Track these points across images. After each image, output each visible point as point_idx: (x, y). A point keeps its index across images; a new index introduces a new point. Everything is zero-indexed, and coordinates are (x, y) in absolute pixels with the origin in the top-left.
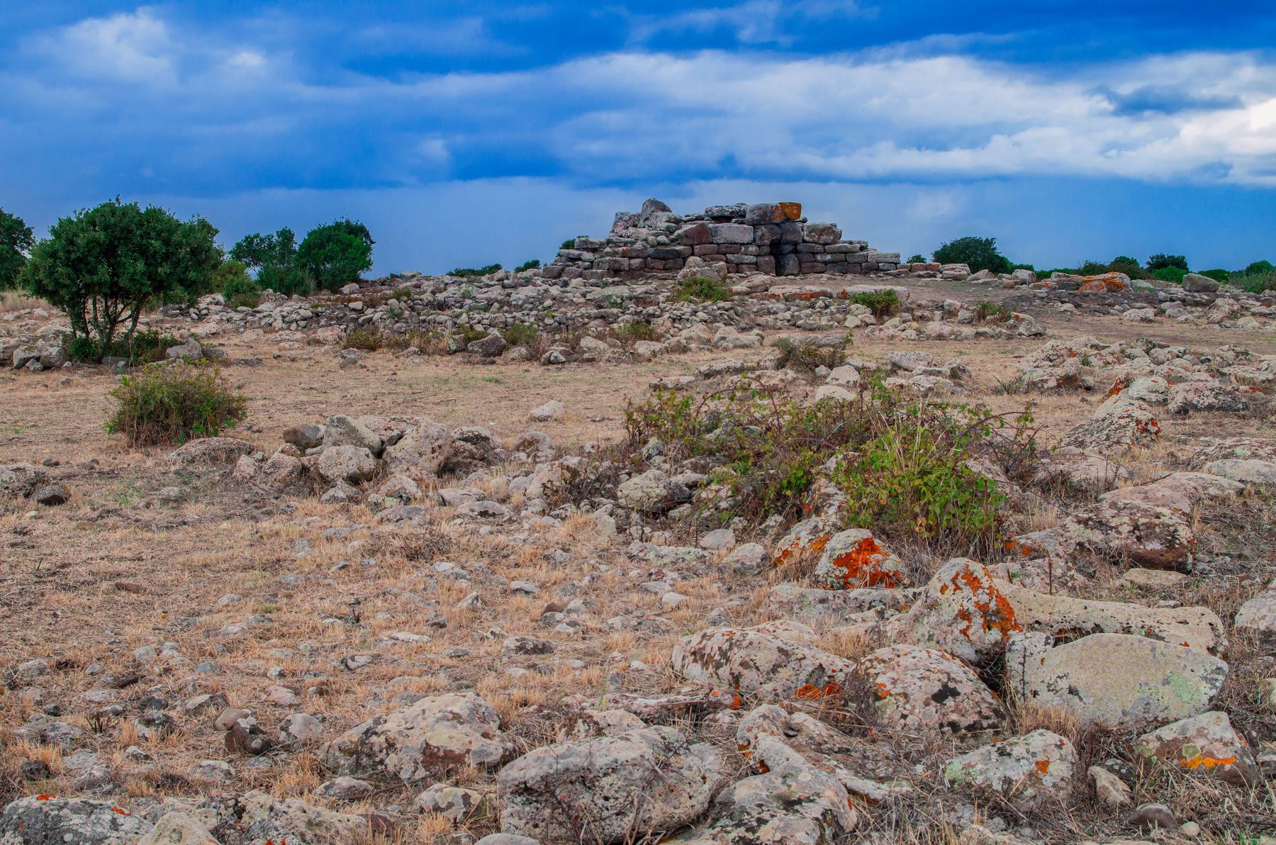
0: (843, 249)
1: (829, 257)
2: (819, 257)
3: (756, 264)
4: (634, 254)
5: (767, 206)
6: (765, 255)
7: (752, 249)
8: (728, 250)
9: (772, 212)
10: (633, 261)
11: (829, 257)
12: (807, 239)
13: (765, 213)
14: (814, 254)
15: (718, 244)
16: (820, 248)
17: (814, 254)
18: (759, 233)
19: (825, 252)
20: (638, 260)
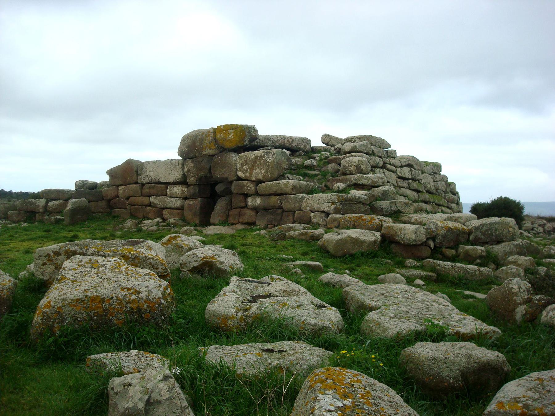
0: (274, 189)
1: (258, 201)
2: (250, 201)
3: (181, 208)
4: (53, 196)
5: (198, 131)
6: (192, 197)
7: (177, 189)
8: (153, 191)
9: (202, 140)
10: (51, 204)
11: (258, 201)
12: (240, 174)
13: (194, 142)
14: (247, 196)
15: (143, 185)
16: (251, 187)
17: (247, 196)
18: (185, 170)
19: (257, 194)
20: (57, 202)
